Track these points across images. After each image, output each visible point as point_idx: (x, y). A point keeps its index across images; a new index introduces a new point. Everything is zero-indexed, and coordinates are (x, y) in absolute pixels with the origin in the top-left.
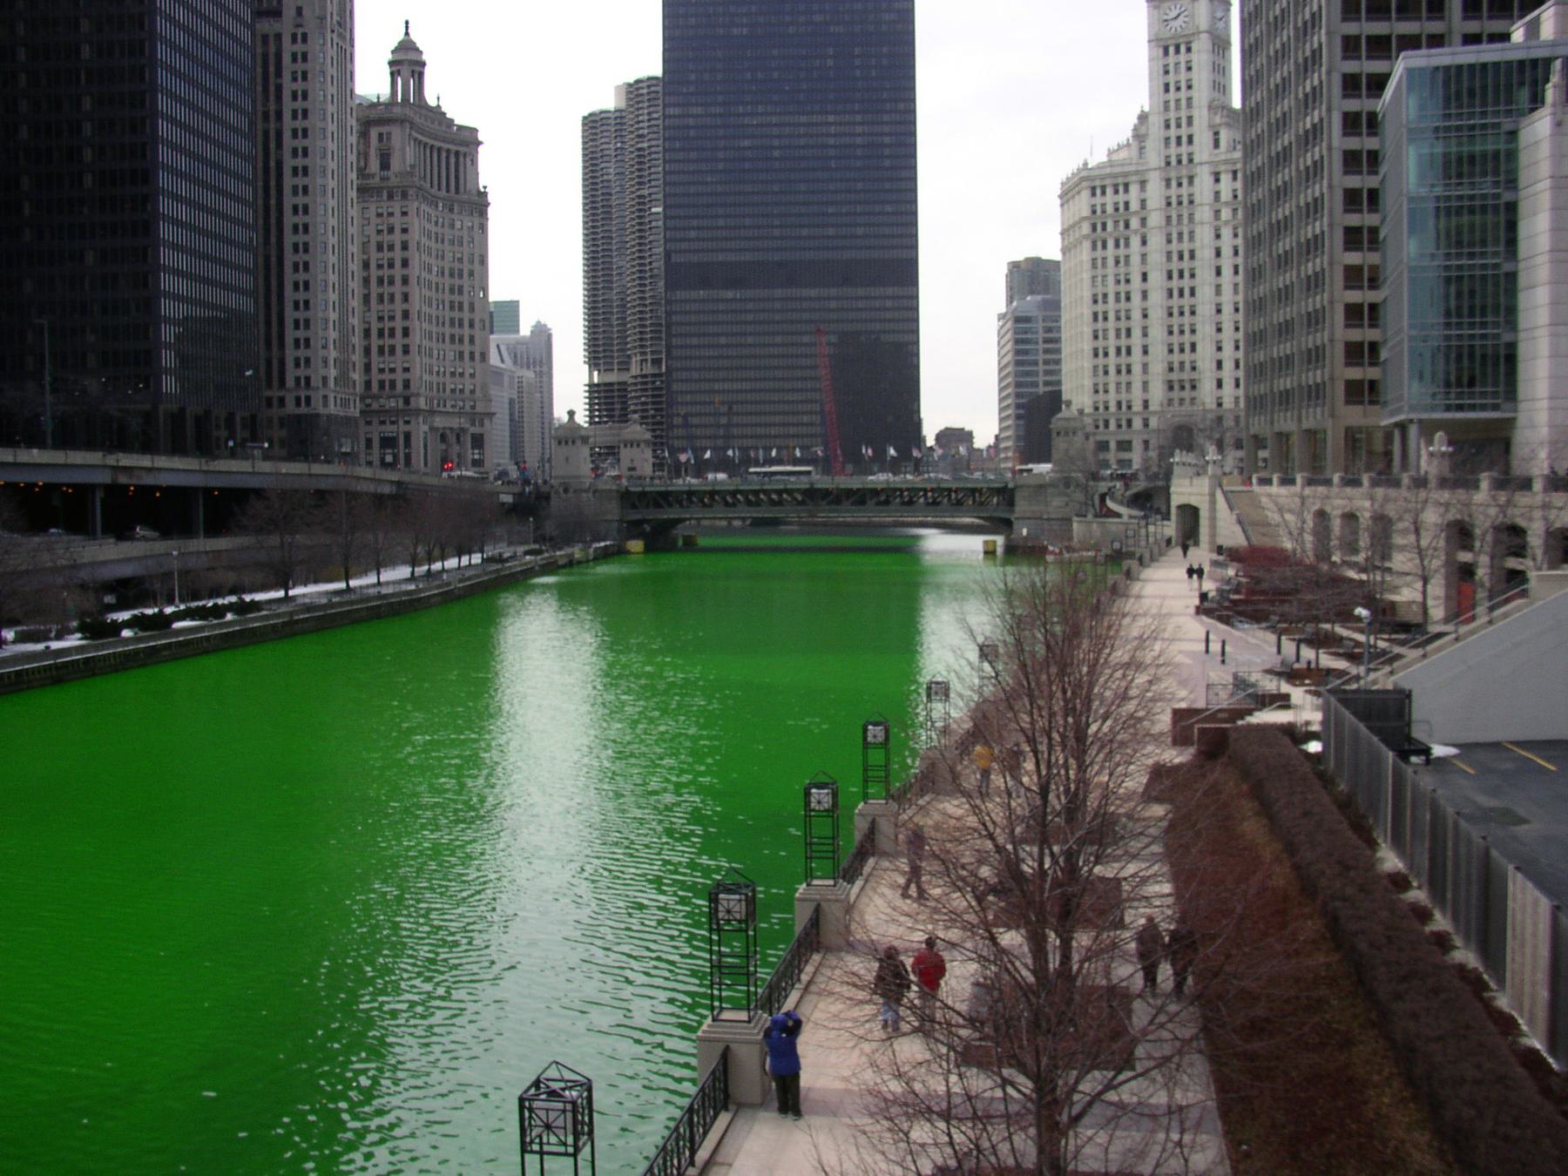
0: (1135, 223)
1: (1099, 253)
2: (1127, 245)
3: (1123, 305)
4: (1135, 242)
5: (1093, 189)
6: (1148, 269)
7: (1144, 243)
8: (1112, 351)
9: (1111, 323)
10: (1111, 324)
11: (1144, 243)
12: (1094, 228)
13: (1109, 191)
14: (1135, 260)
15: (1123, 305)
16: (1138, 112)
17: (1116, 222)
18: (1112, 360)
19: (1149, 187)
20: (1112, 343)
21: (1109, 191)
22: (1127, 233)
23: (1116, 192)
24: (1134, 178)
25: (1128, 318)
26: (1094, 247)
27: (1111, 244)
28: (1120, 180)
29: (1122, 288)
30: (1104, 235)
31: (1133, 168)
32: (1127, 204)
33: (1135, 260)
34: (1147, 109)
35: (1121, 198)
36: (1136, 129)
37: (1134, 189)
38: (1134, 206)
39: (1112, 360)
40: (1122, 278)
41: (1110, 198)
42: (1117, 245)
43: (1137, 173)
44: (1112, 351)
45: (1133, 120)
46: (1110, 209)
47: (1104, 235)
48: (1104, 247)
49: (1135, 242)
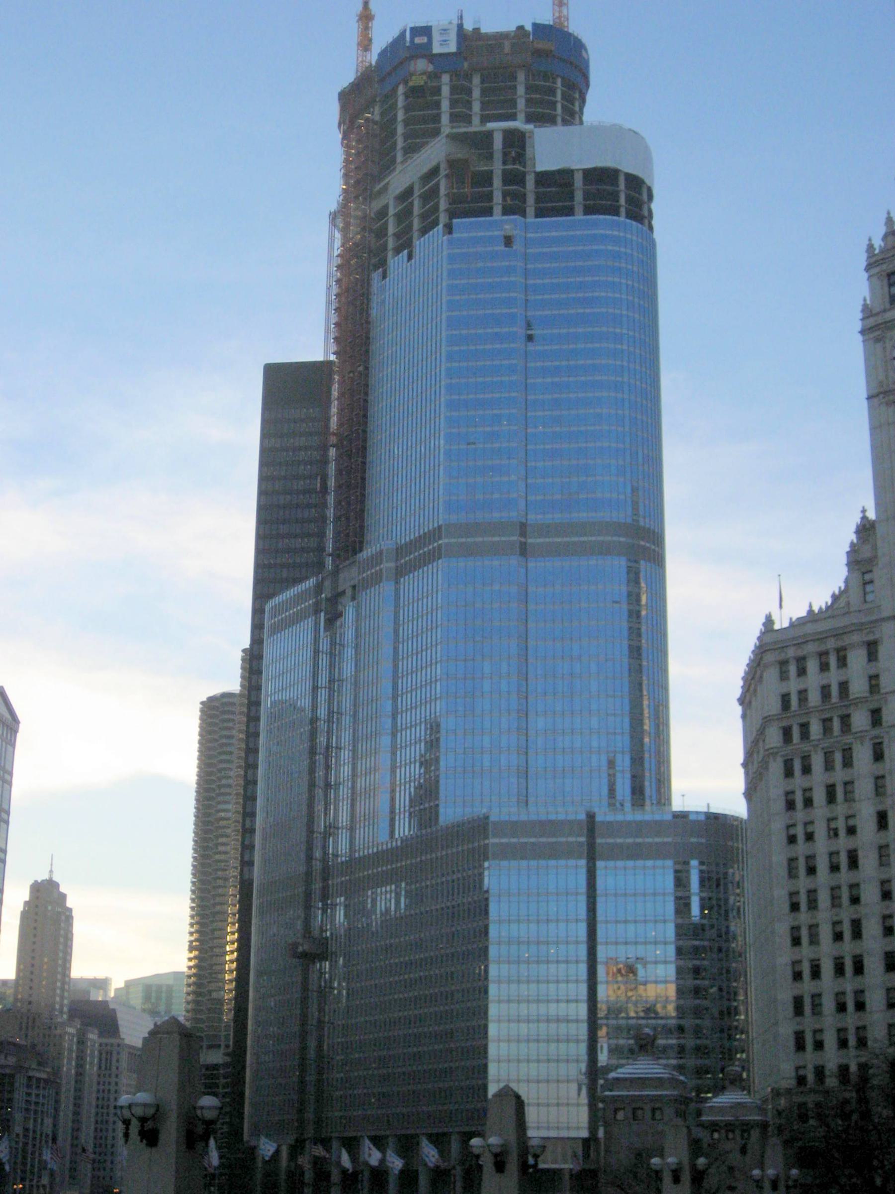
0: (860, 720)
1: (799, 781)
2: (848, 763)
3: (845, 876)
4: (863, 754)
5: (783, 663)
6: (888, 804)
7: (878, 756)
8: (827, 968)
9: (824, 916)
10: (824, 916)
11: (878, 756)
12: (787, 733)
13: (812, 666)
14: (864, 787)
15: (845, 876)
16: (857, 519)
17: (826, 723)
18: (828, 981)
19: (883, 651)
20: (826, 950)
21: (812, 666)
22: (848, 739)
23: (824, 667)
24: (856, 638)
25: (855, 900)
26: (789, 773)
27: (817, 761)
28: (831, 644)
29: (843, 843)
30: (806, 747)
31: (854, 619)
32: (844, 687)
33: (864, 787)
34: (871, 515)
35: (834, 677)
36: (854, 551)
37: (857, 659)
38: (858, 687)
39: (828, 981)
40: (841, 825)
41: (814, 679)
42: (829, 766)
43: (860, 628)
44: (827, 968)
45: (849, 536)
46: (814, 698)
47: (806, 747)
48: (807, 770)
49: (863, 754)
